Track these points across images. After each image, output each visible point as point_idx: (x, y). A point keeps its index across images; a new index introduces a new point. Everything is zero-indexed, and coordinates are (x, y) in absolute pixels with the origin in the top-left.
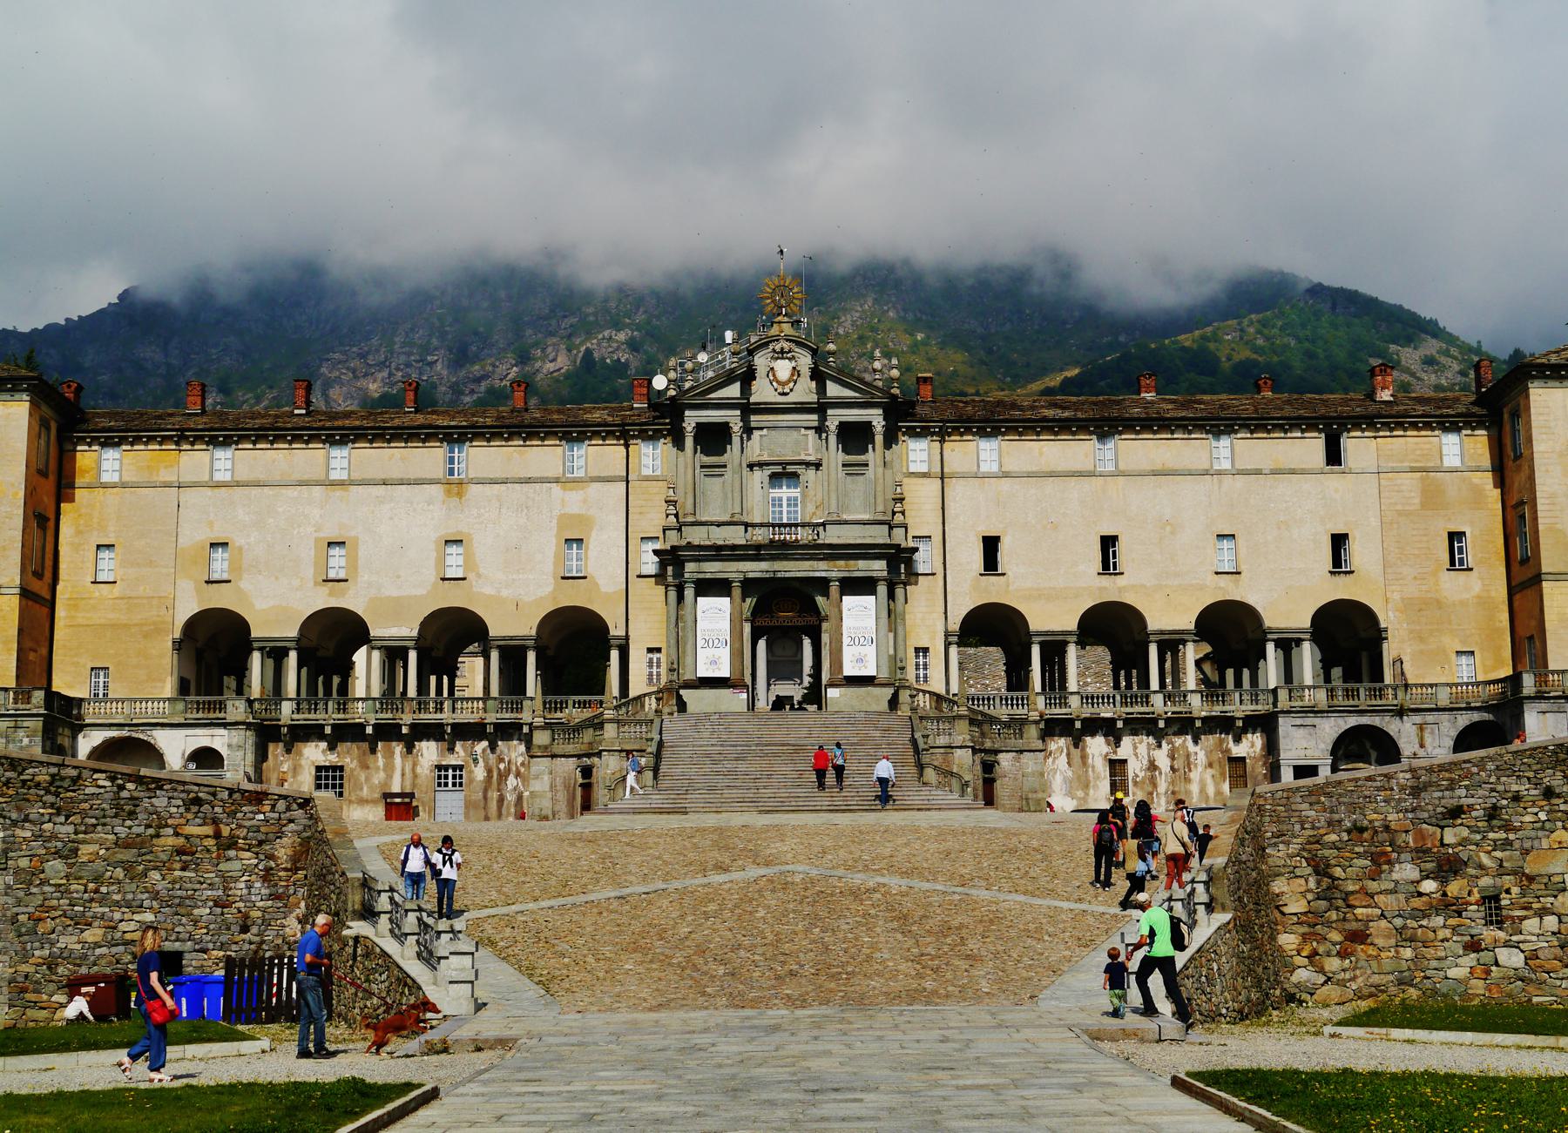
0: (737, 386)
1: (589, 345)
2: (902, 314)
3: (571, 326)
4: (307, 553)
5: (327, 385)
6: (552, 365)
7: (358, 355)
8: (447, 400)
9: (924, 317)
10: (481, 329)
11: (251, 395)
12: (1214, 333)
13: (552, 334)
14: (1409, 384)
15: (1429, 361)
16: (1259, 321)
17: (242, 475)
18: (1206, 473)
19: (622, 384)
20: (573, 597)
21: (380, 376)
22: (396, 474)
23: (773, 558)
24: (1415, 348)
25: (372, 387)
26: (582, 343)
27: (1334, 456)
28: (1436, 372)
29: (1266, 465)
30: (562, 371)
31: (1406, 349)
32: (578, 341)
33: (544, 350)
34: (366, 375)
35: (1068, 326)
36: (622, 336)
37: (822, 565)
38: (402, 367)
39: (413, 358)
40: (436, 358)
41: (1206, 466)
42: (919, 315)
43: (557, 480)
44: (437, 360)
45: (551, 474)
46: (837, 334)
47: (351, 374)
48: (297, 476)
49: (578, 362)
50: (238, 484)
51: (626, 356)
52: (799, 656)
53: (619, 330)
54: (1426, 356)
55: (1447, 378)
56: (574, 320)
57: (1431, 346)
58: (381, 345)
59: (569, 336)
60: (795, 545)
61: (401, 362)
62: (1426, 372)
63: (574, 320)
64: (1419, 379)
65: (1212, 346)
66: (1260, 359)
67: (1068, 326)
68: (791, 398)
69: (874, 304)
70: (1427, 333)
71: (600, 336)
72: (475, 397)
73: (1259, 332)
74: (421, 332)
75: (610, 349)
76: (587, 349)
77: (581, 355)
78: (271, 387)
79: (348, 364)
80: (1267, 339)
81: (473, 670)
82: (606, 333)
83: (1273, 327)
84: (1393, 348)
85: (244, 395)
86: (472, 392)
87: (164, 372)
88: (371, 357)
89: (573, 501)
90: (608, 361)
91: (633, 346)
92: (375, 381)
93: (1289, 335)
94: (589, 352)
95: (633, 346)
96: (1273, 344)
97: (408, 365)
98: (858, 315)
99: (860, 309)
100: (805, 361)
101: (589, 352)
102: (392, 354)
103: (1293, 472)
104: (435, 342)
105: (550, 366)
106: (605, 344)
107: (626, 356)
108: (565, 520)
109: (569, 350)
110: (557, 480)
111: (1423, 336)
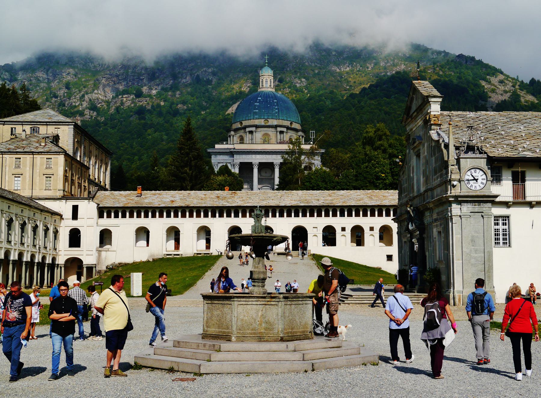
1: (198, 73)
2: (310, 63)
3: (192, 66)
5: (104, 86)
6: (185, 80)
7: (116, 76)
8: (147, 92)
9: (318, 65)
10: (160, 68)
11: (77, 90)
12: (424, 69)
13: (184, 69)
14: (495, 89)
15: (501, 82)
16: (440, 66)
19: (210, 87)
21: (123, 83)
24: (495, 77)
25: (120, 87)
26: (195, 73)
28: (504, 86)
30: (188, 82)
31: (492, 78)
32: (194, 72)
33: (182, 75)
34: (118, 83)
35: (369, 69)
36: (210, 70)
38: (131, 80)
39: (135, 77)
40: (143, 77)
42: (316, 64)
44: (144, 78)
46: (287, 70)
47: (113, 83)
49: (194, 79)
51: (211, 77)
52: (273, 177)
53: (209, 68)
54: (500, 80)
55: (508, 88)
56: (193, 64)
57: (501, 77)
58: (124, 72)
59: (191, 70)
61: (131, 79)
62: (500, 85)
63: (193, 64)
64: (498, 88)
65: (423, 74)
66: (442, 79)
67: (369, 69)
69: (300, 60)
70: (499, 72)
71: (202, 70)
72: (157, 91)
73: (440, 70)
74: (138, 68)
75: (206, 75)
76: (197, 74)
77: (195, 77)
78: (84, 87)
79: (112, 79)
80: (443, 72)
81: (57, 164)
82: (204, 69)
83: (446, 68)
84: (488, 77)
85: (75, 90)
86: (156, 89)
87: (47, 82)
88: (120, 77)
90: (205, 79)
91: (214, 74)
92: (121, 85)
93: (451, 71)
94: (198, 76)
95: (214, 74)
96: (445, 74)
97: (133, 80)
98: (294, 63)
99: (295, 61)
101: (198, 76)
102: (128, 76)
104: (143, 72)
105: (184, 80)
106: (204, 73)
107: (211, 77)
109: (191, 75)
111: (498, 73)
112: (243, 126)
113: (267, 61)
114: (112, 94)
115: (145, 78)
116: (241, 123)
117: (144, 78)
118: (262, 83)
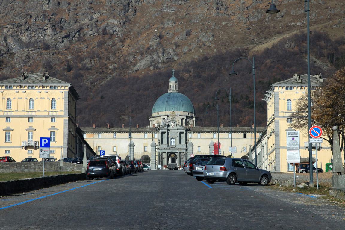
0: (167, 127)
4: (111, 148)
6: (91, 32)
17: (102, 137)
18: (227, 138)
20: (146, 154)
22: (122, 137)
23: (171, 149)
25: (24, 38)
27: (245, 136)
29: (235, 138)
37: (177, 150)
40: (47, 28)
41: (228, 138)
43: (143, 139)
44: (48, 29)
45: (142, 138)
48: (109, 138)
50: (102, 139)
60: (174, 148)
61: (34, 29)
68: (174, 128)
89: (145, 141)
100: (176, 124)
103: (239, 139)
108: (144, 144)
110: (143, 139)
112: (159, 115)
113: (173, 73)
114: (14, 45)
115: (49, 29)
116: (158, 113)
117: (48, 29)
118: (171, 88)
